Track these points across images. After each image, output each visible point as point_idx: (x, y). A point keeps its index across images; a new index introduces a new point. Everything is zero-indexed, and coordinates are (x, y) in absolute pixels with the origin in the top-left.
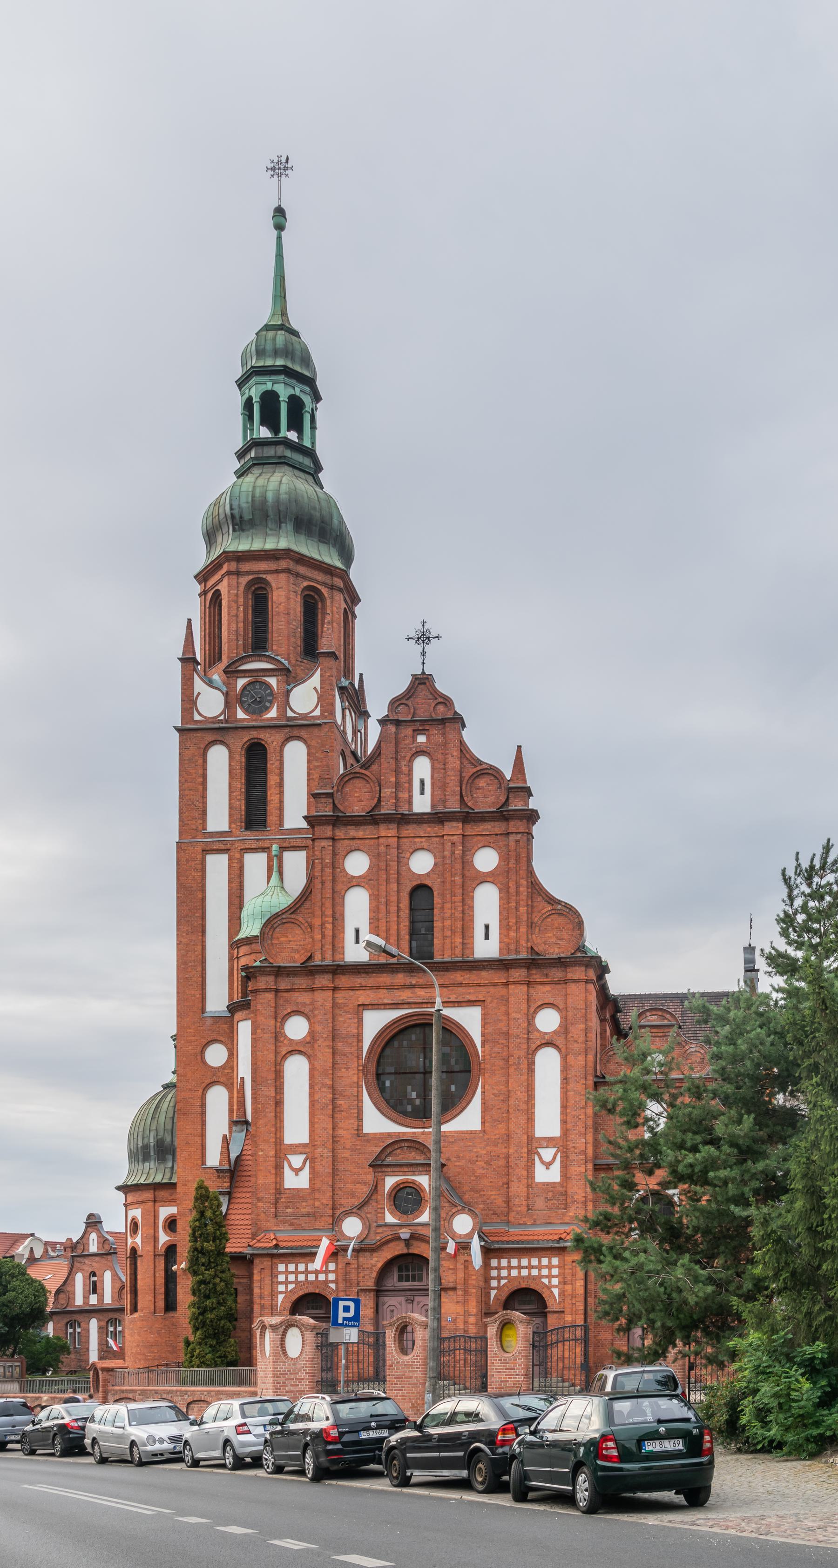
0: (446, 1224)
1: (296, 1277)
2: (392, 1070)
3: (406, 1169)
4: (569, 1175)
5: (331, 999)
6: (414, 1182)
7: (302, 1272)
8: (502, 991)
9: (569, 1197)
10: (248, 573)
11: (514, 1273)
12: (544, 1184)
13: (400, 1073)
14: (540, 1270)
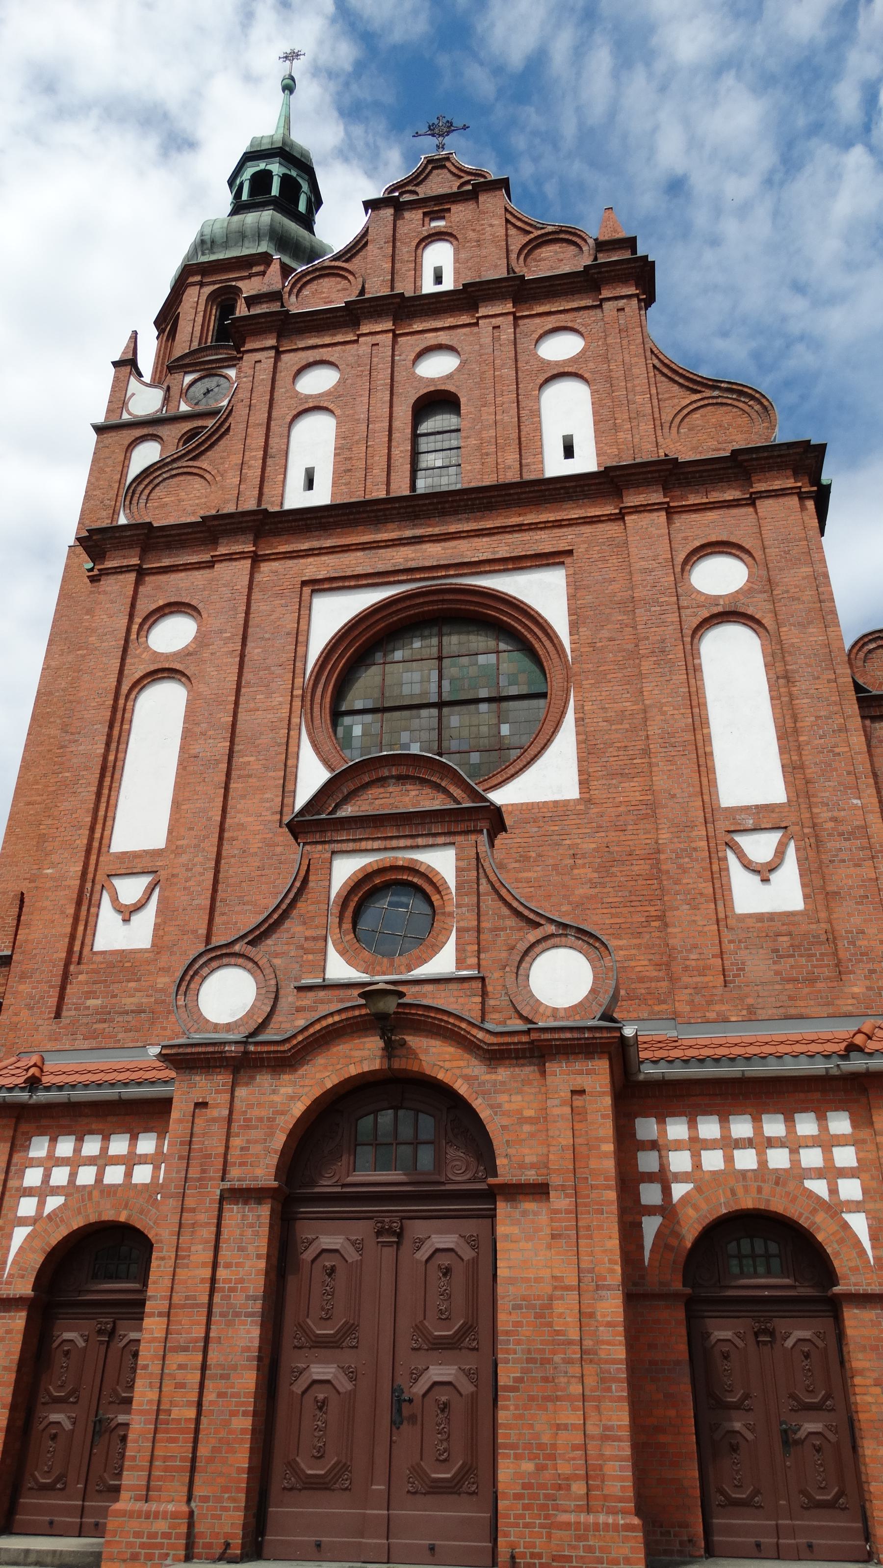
1: (73, 1175)
4: (832, 888)
6: (412, 869)
7: (91, 1161)
8: (612, 529)
9: (843, 944)
10: (214, 283)
11: (713, 1160)
12: (760, 917)
14: (794, 1151)
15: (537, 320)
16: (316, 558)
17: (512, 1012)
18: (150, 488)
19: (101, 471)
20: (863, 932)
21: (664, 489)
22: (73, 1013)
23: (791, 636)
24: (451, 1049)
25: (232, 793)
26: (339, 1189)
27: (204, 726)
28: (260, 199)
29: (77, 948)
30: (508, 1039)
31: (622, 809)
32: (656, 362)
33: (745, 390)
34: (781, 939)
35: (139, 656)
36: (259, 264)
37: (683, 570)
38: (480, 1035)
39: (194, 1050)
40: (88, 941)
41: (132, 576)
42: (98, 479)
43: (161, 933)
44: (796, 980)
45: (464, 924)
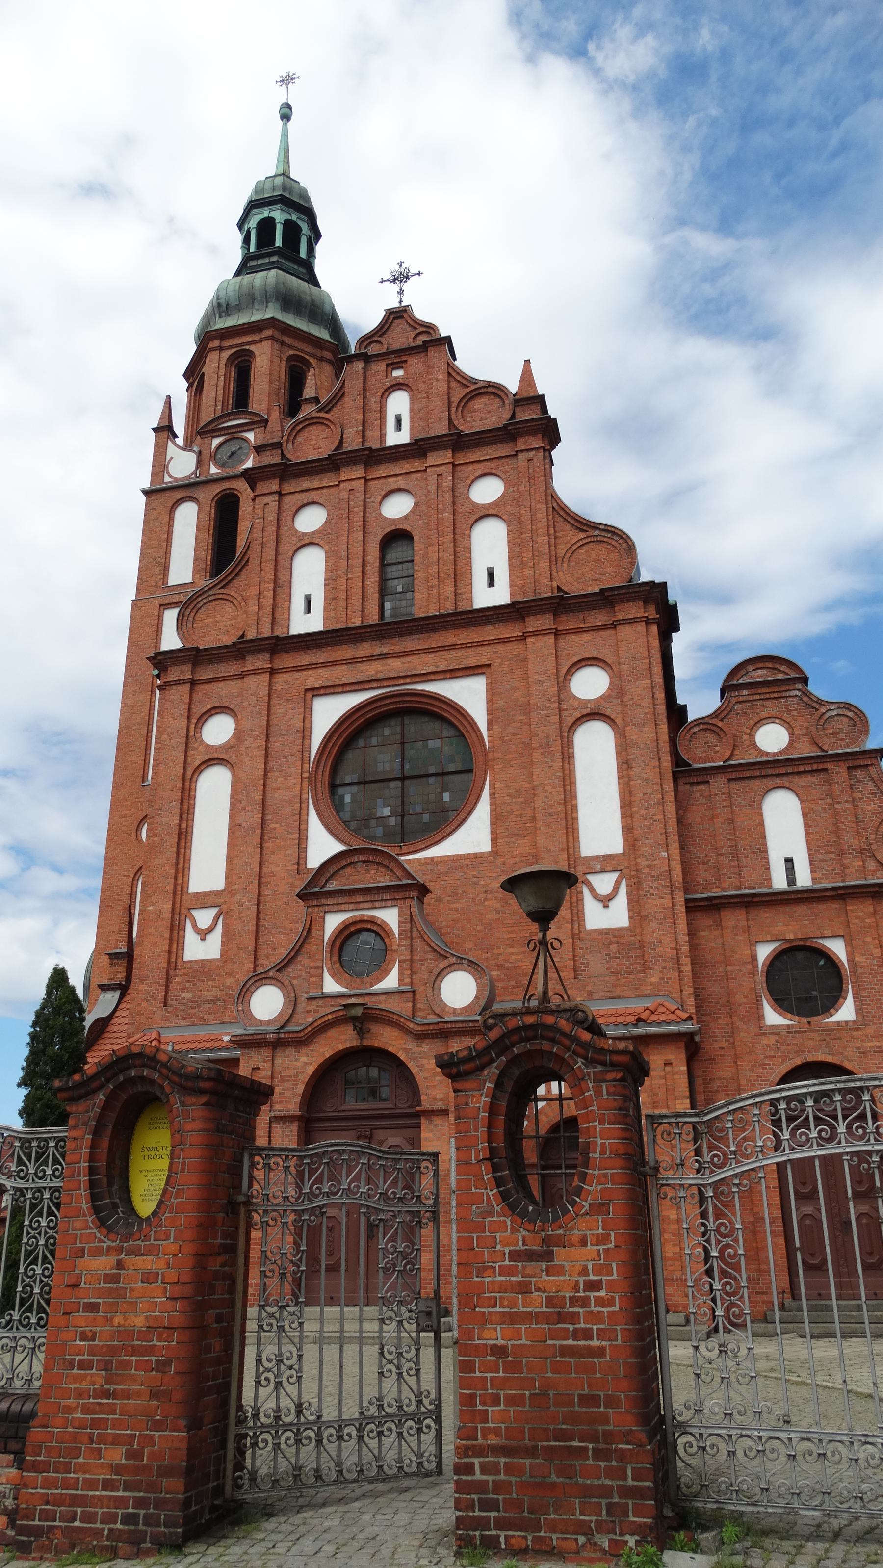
0: (429, 991)
2: (354, 778)
3: (360, 898)
4: (644, 913)
5: (267, 684)
6: (372, 921)
8: (516, 648)
10: (231, 347)
12: (601, 932)
13: (366, 783)
15: (471, 467)
16: (315, 671)
17: (430, 1011)
18: (194, 611)
19: (152, 532)
20: (660, 942)
21: (554, 615)
22: (174, 1002)
23: (632, 732)
24: (396, 1034)
25: (265, 851)
26: (336, 1114)
27: (244, 803)
28: (265, 251)
29: (173, 960)
30: (427, 1028)
31: (517, 859)
32: (555, 505)
33: (616, 531)
34: (612, 946)
35: (196, 749)
36: (267, 328)
37: (565, 679)
38: (411, 1026)
39: (249, 1038)
40: (180, 954)
41: (188, 686)
42: (149, 539)
43: (226, 948)
44: (619, 973)
45: (403, 958)
